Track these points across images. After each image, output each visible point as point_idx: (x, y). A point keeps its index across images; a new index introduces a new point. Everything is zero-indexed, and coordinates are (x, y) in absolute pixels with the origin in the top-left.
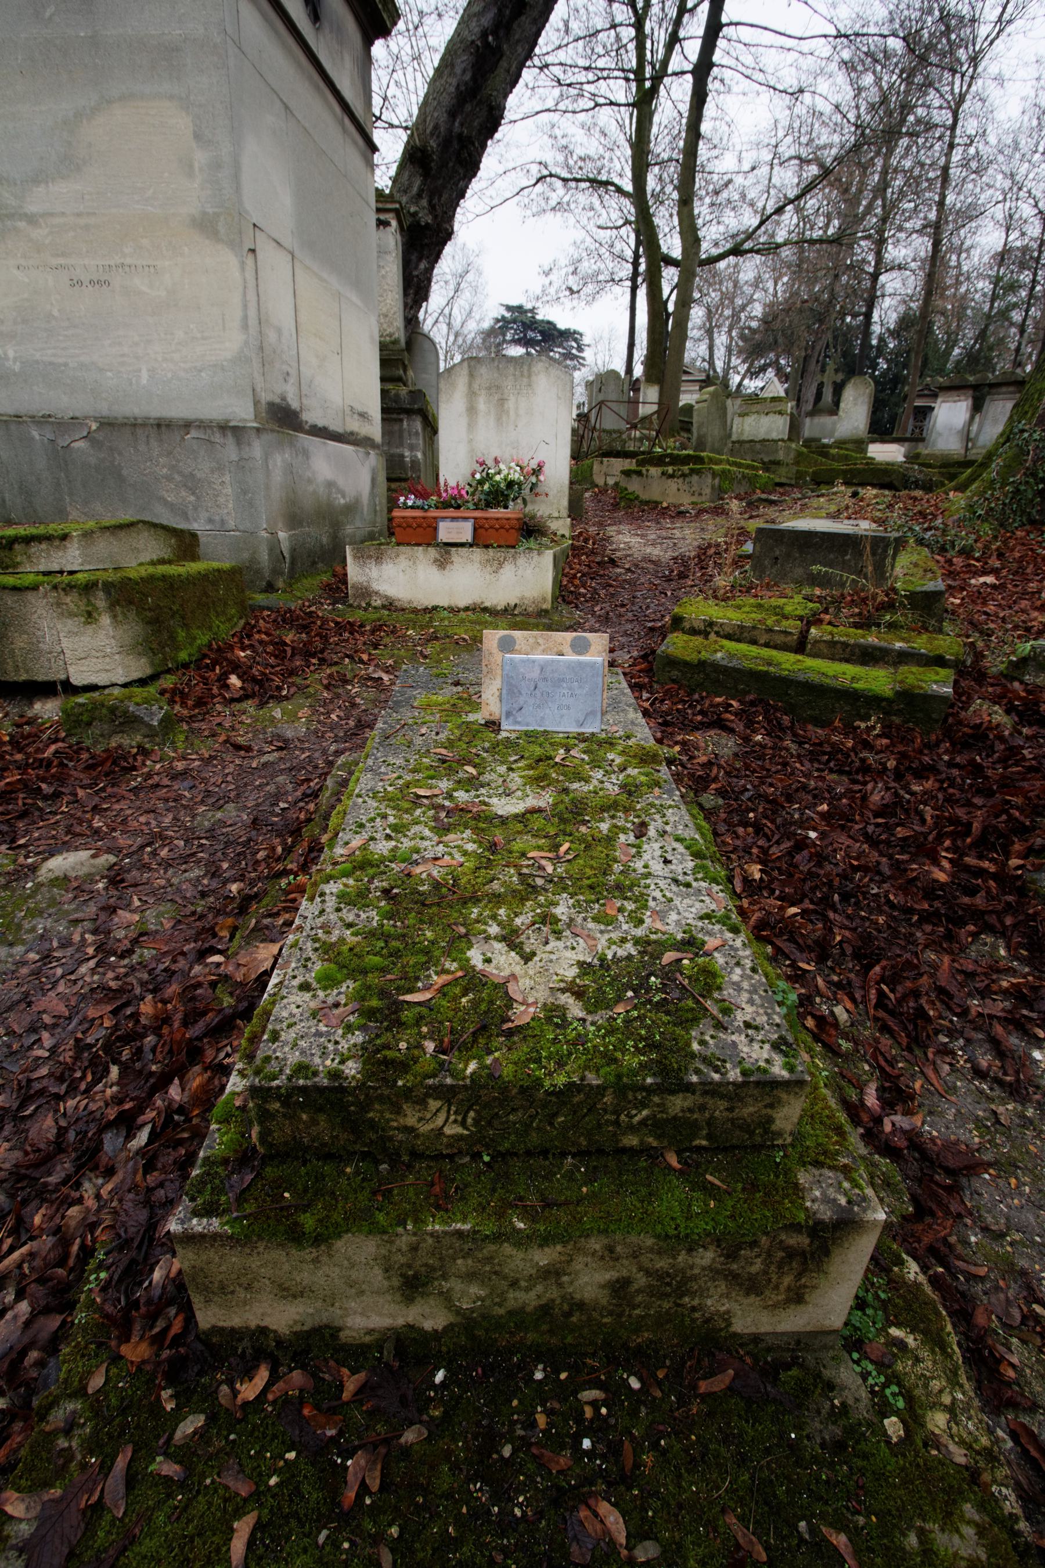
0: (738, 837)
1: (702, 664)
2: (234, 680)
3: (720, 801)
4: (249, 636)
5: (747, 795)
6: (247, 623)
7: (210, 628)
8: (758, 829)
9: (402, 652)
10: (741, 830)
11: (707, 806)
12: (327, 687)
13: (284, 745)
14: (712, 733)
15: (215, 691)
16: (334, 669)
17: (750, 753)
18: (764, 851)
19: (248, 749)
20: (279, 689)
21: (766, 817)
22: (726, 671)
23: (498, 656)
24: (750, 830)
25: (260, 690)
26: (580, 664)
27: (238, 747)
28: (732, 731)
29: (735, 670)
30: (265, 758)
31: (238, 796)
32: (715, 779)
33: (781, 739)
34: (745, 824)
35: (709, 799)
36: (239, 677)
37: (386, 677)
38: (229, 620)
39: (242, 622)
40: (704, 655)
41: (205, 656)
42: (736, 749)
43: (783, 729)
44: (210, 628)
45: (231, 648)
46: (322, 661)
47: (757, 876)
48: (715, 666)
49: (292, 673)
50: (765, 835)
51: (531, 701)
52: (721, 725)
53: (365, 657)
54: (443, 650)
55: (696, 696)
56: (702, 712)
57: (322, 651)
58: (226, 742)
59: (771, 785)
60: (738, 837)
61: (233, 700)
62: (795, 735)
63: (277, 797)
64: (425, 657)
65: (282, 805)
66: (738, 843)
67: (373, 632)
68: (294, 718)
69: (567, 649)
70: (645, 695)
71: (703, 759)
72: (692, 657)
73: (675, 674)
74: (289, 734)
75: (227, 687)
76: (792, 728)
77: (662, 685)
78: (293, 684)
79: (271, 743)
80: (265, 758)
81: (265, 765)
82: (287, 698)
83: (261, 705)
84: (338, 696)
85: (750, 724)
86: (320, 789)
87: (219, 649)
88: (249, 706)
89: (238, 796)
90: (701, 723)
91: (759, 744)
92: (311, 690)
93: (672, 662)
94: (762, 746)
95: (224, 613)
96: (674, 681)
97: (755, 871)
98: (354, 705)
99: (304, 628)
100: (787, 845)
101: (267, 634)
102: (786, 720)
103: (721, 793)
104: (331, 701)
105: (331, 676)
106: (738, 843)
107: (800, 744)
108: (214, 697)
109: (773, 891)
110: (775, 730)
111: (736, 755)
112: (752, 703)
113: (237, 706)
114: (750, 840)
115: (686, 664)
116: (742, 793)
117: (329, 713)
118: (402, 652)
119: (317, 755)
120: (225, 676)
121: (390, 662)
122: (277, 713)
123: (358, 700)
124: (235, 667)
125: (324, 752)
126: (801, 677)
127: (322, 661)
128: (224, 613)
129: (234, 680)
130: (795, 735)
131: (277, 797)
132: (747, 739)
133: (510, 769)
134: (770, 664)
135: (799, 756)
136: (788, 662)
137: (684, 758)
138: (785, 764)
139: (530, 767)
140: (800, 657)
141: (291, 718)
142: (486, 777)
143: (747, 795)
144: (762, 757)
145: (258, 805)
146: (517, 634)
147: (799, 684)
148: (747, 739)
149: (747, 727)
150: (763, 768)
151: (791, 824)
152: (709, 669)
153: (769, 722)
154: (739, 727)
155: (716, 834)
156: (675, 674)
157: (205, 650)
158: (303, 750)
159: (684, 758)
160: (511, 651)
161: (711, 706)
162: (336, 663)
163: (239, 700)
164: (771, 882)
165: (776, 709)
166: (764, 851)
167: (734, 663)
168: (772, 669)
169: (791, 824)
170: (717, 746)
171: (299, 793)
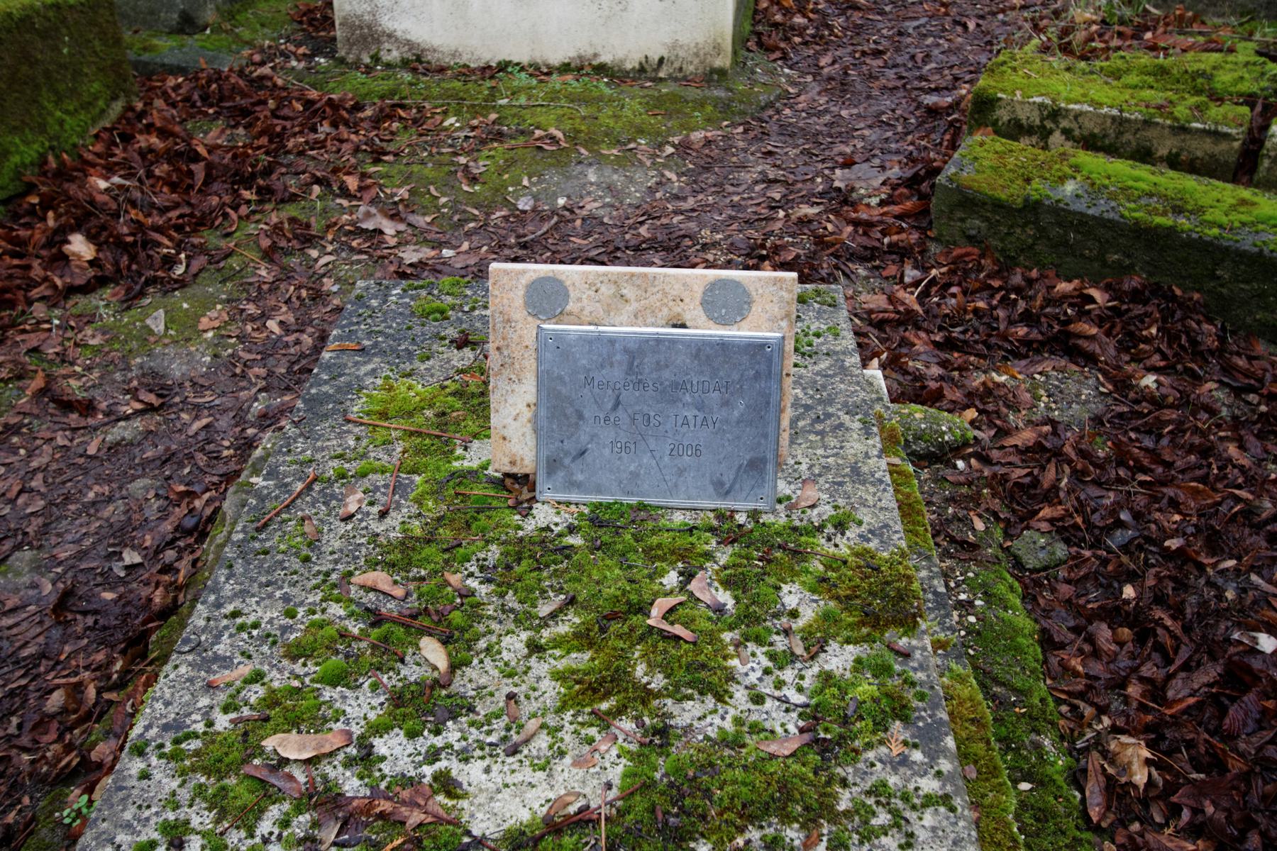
0: (1096, 654)
1: (1032, 208)
2: (79, 246)
3: (1061, 550)
4: (127, 139)
5: (1120, 536)
6: (130, 108)
7: (42, 129)
8: (1144, 632)
9: (429, 170)
10: (1103, 633)
11: (1031, 562)
12: (269, 255)
13: (161, 396)
14: (1047, 366)
15: (37, 271)
16: (291, 210)
17: (1129, 413)
18: (1156, 691)
19: (88, 408)
20: (170, 262)
21: (1159, 600)
22: (1082, 223)
23: (526, 330)
24: (1125, 632)
25: (133, 268)
26: (724, 346)
27: (67, 406)
28: (1091, 359)
29: (1100, 221)
30: (121, 431)
31: (44, 530)
32: (1051, 496)
33: (1197, 379)
34: (1114, 614)
35: (1037, 545)
36: (91, 238)
37: (389, 228)
38: (86, 106)
39: (118, 106)
40: (1037, 189)
41: (30, 188)
42: (1097, 407)
43: (1200, 355)
44: (42, 129)
45: (85, 166)
46: (265, 194)
47: (1140, 777)
48: (1061, 214)
49: (202, 222)
50: (1159, 647)
51: (607, 434)
52: (1066, 346)
53: (352, 182)
54: (510, 163)
55: (1017, 279)
56: (1028, 318)
57: (268, 172)
58: (42, 392)
59: (1174, 504)
60: (1096, 654)
61: (71, 290)
62: (1228, 369)
63: (122, 535)
64: (473, 180)
65: (131, 557)
66: (1097, 668)
67: (376, 122)
68: (186, 329)
69: (693, 312)
70: (911, 274)
71: (1026, 437)
72: (1011, 192)
73: (975, 224)
74: (177, 370)
75: (62, 259)
76: (1220, 352)
77: (948, 244)
78: (202, 249)
79: (134, 393)
80: (121, 431)
81: (114, 449)
82: (182, 283)
83: (131, 300)
84: (287, 275)
85: (1130, 343)
86: (211, 519)
87: (63, 174)
88: (103, 303)
89: (44, 530)
90: (1026, 342)
91: (1145, 396)
92: (234, 263)
93: (968, 201)
94: (1158, 403)
95: (74, 92)
96: (970, 239)
97: (1136, 759)
98: (318, 296)
99: (242, 115)
100: (1209, 673)
101: (164, 133)
102: (1208, 333)
103: (1062, 530)
104: (274, 288)
105: (278, 228)
106: (1097, 668)
107: (1238, 392)
108: (33, 284)
109: (1175, 811)
110: (1183, 358)
111: (1097, 420)
112: (1136, 296)
113: (82, 303)
114: (1124, 662)
115: (998, 205)
116: (1108, 530)
117: (264, 316)
118: (429, 170)
119: (224, 422)
120: (58, 238)
121: (403, 192)
122: (157, 322)
123: (329, 285)
124: (86, 217)
125: (240, 419)
126: (1247, 243)
127: (265, 194)
128: (74, 92)
129: (79, 246)
130: (1228, 369)
131: (122, 535)
132: (1123, 385)
133: (535, 648)
134: (1178, 210)
135: (1236, 424)
136: (1219, 205)
137: (985, 435)
138: (1206, 452)
139: (583, 639)
140: (1246, 193)
141: (184, 333)
142: (464, 683)
143: (1120, 536)
144: (1154, 429)
145: (82, 555)
146: (571, 273)
147: (1241, 256)
148: (1123, 385)
149: (1122, 348)
150: (1154, 455)
151: (1220, 614)
152: (1046, 219)
153: (1173, 338)
154: (1107, 350)
155: (1048, 642)
156: (975, 224)
157: (29, 176)
158: (197, 410)
159: (985, 435)
160: (559, 316)
161: (1048, 302)
162: (293, 198)
163: (86, 289)
164: (1171, 788)
165: (1189, 309)
166: (1156, 691)
167: (1101, 208)
168: (1183, 223)
169: (1220, 614)
170: (1058, 397)
171: (167, 527)
